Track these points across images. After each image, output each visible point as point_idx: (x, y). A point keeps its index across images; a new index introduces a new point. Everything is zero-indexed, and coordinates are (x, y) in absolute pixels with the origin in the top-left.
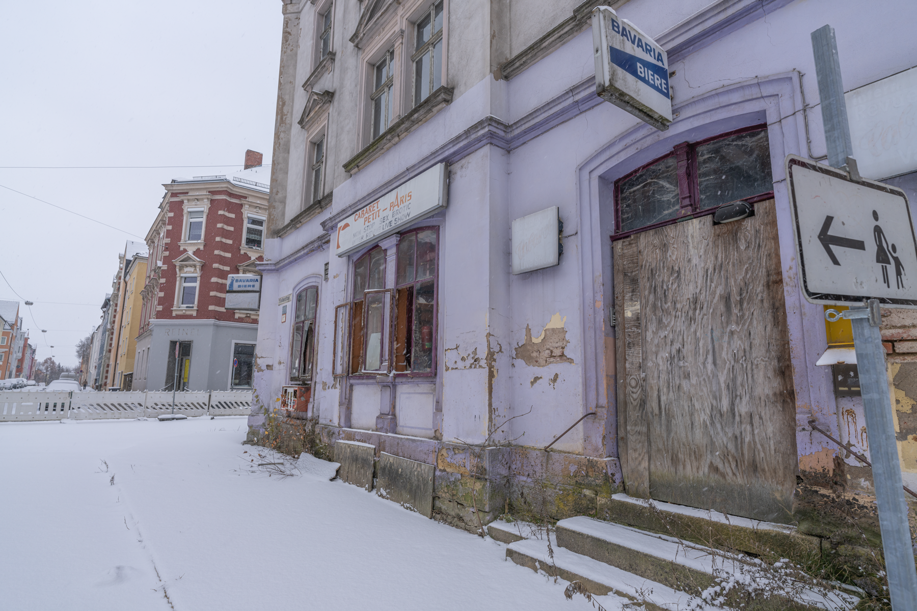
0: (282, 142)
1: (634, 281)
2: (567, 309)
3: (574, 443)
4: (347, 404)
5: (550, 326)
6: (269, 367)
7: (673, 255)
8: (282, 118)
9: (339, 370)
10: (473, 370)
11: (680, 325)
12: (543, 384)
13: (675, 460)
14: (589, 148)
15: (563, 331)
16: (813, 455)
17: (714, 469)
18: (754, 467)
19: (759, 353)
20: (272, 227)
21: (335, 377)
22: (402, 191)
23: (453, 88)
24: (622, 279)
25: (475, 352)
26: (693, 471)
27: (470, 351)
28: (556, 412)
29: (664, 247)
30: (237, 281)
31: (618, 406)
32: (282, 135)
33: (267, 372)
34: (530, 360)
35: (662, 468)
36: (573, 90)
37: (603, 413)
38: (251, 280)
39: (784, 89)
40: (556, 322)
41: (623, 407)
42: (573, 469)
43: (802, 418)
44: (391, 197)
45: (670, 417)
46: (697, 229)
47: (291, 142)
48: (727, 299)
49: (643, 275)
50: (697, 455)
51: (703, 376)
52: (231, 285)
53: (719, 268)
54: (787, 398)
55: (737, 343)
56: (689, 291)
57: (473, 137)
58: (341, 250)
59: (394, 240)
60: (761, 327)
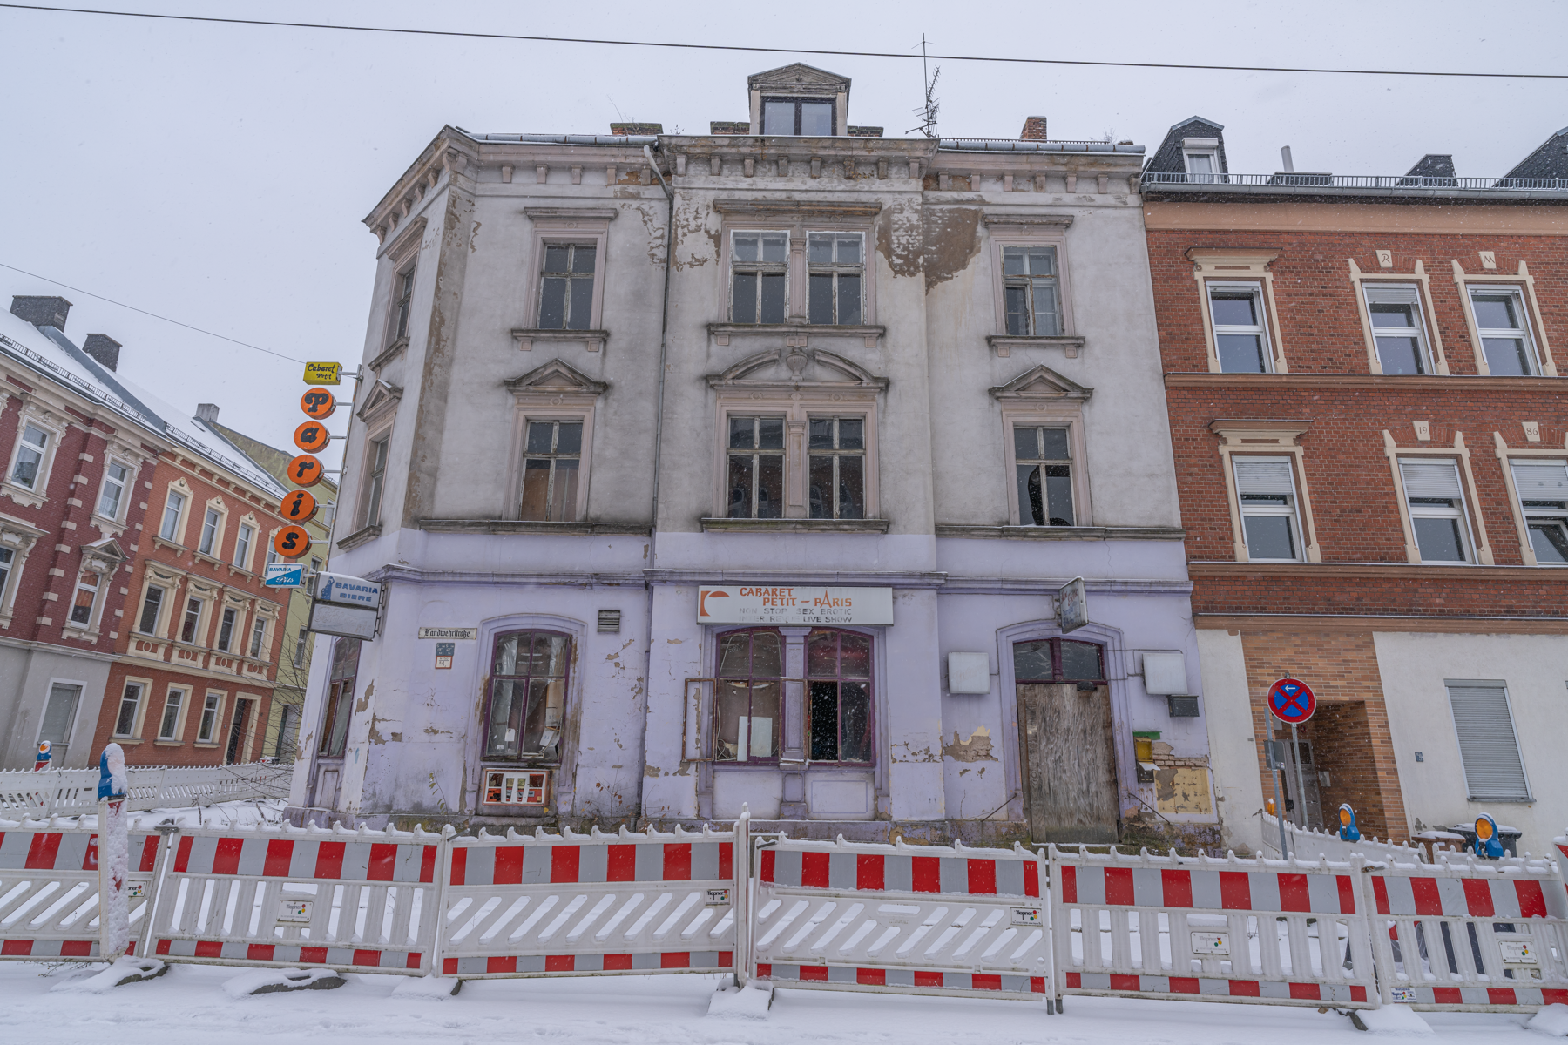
0: (436, 381)
1: (1033, 713)
2: (991, 723)
3: (1002, 815)
4: (705, 791)
5: (976, 734)
6: (396, 737)
7: (1055, 702)
8: (438, 343)
9: (693, 752)
10: (927, 764)
11: (1060, 742)
12: (972, 775)
13: (1059, 819)
14: (1006, 620)
15: (988, 739)
16: (1128, 809)
17: (1080, 821)
18: (1099, 818)
19: (1099, 762)
20: (414, 511)
21: (686, 762)
22: (834, 593)
23: (888, 524)
24: (1025, 711)
25: (928, 749)
26: (1068, 824)
27: (923, 748)
28: (987, 791)
29: (1051, 696)
30: (338, 585)
31: (1027, 788)
32: (436, 370)
33: (392, 746)
34: (958, 757)
35: (1053, 824)
36: (1003, 581)
37: (1020, 793)
38: (365, 589)
39: (1116, 637)
40: (981, 732)
41: (1030, 789)
42: (1004, 831)
43: (1123, 792)
44: (819, 592)
45: (1055, 794)
46: (1068, 689)
47: (452, 388)
48: (1084, 731)
49: (1038, 710)
50: (1071, 815)
51: (1072, 772)
52: (328, 590)
53: (1081, 714)
54: (1114, 783)
55: (1090, 756)
56: (1065, 724)
57: (927, 580)
58: (702, 619)
60: (1101, 750)
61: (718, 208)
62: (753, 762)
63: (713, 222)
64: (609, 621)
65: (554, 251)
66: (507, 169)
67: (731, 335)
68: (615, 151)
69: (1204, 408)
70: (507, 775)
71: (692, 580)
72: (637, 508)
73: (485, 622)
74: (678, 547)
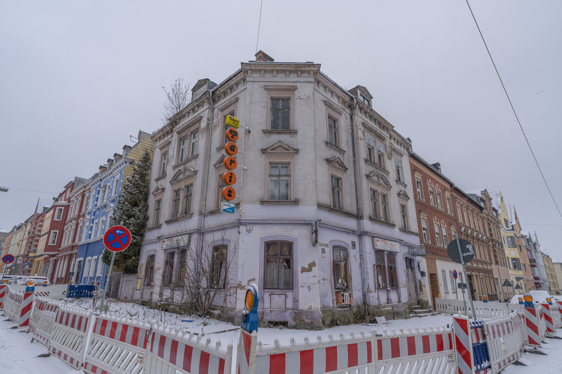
59: (387, 253)
61: (363, 124)
62: (383, 288)
63: (362, 127)
64: (354, 245)
65: (274, 100)
67: (369, 164)
68: (344, 94)
69: (421, 207)
70: (345, 294)
72: (354, 210)
73: (331, 242)
74: (368, 225)
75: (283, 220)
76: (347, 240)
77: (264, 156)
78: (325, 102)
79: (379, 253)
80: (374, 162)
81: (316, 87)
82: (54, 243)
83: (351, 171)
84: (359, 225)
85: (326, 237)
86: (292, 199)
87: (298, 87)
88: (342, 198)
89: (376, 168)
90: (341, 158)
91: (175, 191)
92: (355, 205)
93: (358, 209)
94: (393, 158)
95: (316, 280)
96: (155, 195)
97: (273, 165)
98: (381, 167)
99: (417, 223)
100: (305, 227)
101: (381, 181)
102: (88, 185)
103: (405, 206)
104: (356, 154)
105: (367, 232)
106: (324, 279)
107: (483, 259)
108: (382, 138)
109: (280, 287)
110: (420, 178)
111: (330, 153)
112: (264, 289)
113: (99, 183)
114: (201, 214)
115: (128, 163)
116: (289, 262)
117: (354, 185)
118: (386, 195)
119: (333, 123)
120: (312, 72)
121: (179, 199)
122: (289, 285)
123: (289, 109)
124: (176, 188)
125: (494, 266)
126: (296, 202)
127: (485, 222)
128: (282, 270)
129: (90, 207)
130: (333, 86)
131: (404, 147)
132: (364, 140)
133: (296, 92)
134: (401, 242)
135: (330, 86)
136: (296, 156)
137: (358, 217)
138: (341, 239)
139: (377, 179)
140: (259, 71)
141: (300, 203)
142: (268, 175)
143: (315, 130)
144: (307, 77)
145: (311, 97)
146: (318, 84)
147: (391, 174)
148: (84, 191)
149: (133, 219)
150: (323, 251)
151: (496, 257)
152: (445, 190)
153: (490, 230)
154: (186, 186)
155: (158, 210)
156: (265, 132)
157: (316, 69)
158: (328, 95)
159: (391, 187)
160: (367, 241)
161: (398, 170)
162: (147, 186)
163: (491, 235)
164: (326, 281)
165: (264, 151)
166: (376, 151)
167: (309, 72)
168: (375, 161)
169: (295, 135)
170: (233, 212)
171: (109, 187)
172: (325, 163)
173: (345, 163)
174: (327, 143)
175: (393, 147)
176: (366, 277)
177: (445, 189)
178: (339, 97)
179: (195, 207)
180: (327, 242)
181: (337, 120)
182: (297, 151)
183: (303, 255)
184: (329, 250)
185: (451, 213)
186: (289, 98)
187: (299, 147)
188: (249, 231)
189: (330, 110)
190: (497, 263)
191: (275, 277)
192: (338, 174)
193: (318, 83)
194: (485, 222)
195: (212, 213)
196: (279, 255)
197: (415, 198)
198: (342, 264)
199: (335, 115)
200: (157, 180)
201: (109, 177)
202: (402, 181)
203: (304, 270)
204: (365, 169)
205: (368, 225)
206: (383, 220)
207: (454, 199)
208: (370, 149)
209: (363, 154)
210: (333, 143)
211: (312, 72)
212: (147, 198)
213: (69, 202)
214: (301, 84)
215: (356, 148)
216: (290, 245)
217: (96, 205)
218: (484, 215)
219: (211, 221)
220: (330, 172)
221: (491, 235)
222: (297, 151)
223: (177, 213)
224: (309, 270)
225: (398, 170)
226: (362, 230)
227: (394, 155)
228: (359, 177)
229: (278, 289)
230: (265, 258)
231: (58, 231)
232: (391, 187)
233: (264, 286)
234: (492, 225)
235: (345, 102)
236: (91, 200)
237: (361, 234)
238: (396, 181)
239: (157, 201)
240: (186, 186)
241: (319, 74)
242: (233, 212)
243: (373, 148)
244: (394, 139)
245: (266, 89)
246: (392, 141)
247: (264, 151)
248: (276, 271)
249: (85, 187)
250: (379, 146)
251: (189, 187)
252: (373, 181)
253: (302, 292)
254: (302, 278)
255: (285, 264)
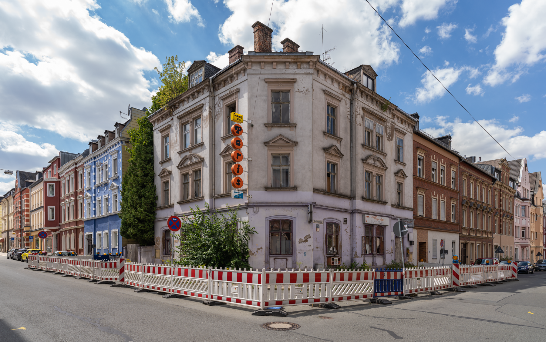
66: (287, 64)
67: (366, 148)
71: (363, 213)
72: (348, 192)
73: (325, 219)
74: (359, 204)
75: (284, 203)
76: (339, 217)
77: (266, 148)
78: (324, 91)
79: (368, 227)
80: (372, 145)
81: (315, 76)
82: (53, 218)
83: (347, 156)
84: (351, 204)
85: (320, 216)
86: (292, 185)
87: (298, 80)
88: (337, 181)
89: (373, 151)
90: (338, 145)
91: (183, 175)
92: (349, 187)
93: (351, 190)
94: (394, 139)
95: (311, 248)
96: (162, 177)
97: (275, 157)
98: (380, 149)
99: (412, 199)
100: (303, 208)
101: (378, 164)
102: (80, 161)
103: (402, 184)
104: (354, 140)
105: (358, 210)
106: (317, 248)
107: (484, 228)
108: (382, 120)
109: (282, 253)
110: (423, 155)
111: (328, 142)
112: (270, 254)
113: (93, 160)
114: (211, 196)
115: (124, 142)
116: (289, 236)
117: (349, 169)
118: (382, 176)
119: (331, 111)
120: (311, 63)
121: (188, 182)
122: (290, 252)
123: (289, 102)
124: (185, 171)
125: (496, 236)
126: (295, 188)
127: (496, 193)
128: (284, 242)
129: (87, 186)
130: (333, 73)
131: (409, 124)
132: (363, 124)
133: (296, 85)
134: (391, 217)
135: (330, 73)
136: (295, 148)
137: (352, 197)
138: (334, 217)
139: (373, 162)
140: (259, 62)
141: (298, 189)
142: (270, 165)
143: (314, 122)
144: (306, 68)
145: (311, 90)
146: (318, 73)
147: (388, 156)
148: (76, 168)
149: (143, 199)
150: (318, 227)
151: (500, 226)
152: (451, 165)
153: (500, 200)
154: (193, 171)
155: (167, 191)
156: (267, 125)
157: (315, 60)
158: (328, 82)
159: (387, 168)
160: (358, 218)
161: (399, 150)
162: (152, 169)
163: (500, 206)
164: (319, 249)
165: (266, 144)
166: (374, 134)
167: (308, 63)
168: (373, 144)
169: (294, 128)
170: (242, 198)
171: (107, 165)
172: (322, 153)
173: (342, 151)
174: (324, 133)
175: (396, 126)
176: (354, 246)
177: (451, 164)
178: (339, 83)
179: (206, 189)
180: (322, 220)
181: (336, 107)
182: (296, 144)
183: (301, 230)
184: (323, 227)
185: (455, 187)
186: (289, 91)
187: (298, 140)
188: (256, 212)
189: (329, 98)
190: (500, 232)
191: (278, 246)
192: (334, 160)
193: (318, 71)
194: (496, 193)
195: (222, 196)
196: (281, 230)
197: (414, 175)
198: (334, 236)
199: (334, 102)
200: (162, 163)
201: (104, 155)
202: (401, 160)
203: (301, 241)
204: (361, 153)
205: (359, 204)
206: (375, 198)
207: (460, 173)
208: (369, 133)
209: (361, 137)
210: (331, 131)
211: (311, 63)
212: (153, 180)
213: (59, 178)
214: (301, 76)
215: (354, 134)
216: (289, 223)
217: (95, 183)
218: (496, 186)
219: (223, 204)
220: (327, 159)
221: (500, 206)
222: (296, 144)
223: (188, 195)
224: (306, 241)
225: (399, 150)
226: (354, 209)
227: (396, 135)
228: (354, 162)
229: (280, 254)
230: (270, 232)
231: (54, 207)
232: (387, 168)
233: (270, 252)
234: (504, 196)
235: (346, 87)
236: (86, 178)
237: (353, 212)
238: (395, 160)
239: (164, 182)
240: (193, 171)
241: (318, 63)
242: (242, 198)
243: (372, 131)
244: (398, 118)
245: (267, 81)
246: (396, 120)
247: (266, 144)
248: (278, 242)
249: (76, 164)
250: (378, 128)
251: (197, 173)
252: (369, 164)
253: (300, 257)
254: (299, 247)
255: (286, 236)
